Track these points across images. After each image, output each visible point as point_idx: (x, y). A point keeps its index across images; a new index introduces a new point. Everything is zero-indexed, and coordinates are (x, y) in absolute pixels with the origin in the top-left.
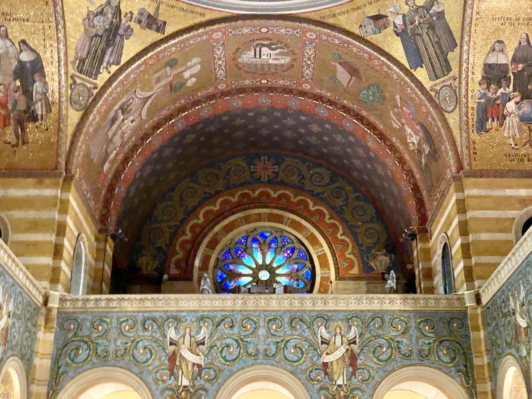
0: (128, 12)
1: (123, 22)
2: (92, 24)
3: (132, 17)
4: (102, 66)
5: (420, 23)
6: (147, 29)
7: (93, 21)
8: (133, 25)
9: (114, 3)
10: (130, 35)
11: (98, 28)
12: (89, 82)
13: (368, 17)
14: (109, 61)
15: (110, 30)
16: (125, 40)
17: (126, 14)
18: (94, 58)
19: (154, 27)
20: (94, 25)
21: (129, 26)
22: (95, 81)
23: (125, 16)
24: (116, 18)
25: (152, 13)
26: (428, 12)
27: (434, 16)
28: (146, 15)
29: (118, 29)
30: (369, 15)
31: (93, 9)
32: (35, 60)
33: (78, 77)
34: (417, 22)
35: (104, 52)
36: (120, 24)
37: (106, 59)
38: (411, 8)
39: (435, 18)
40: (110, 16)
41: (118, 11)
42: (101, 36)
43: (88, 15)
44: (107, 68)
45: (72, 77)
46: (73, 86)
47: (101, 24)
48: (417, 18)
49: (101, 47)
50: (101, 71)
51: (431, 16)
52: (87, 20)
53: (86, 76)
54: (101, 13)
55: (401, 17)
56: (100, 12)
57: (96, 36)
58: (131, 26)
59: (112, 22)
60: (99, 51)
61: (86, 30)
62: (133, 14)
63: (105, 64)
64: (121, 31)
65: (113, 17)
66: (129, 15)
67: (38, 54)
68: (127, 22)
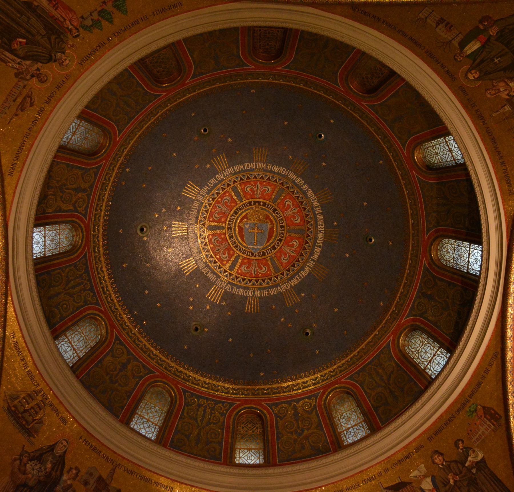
0: (73, 466)
1: (65, 477)
2: (22, 468)
5: (455, 482)
7: (25, 465)
9: (58, 451)
11: (30, 476)
13: (386, 488)
20: (25, 470)
24: (56, 471)
25: (105, 477)
26: (464, 466)
27: (472, 468)
29: (56, 486)
30: (387, 485)
31: (29, 449)
34: (452, 481)
36: (59, 480)
38: (441, 466)
39: (474, 471)
40: (49, 465)
41: (60, 462)
43: (21, 455)
48: (450, 476)
51: (469, 469)
54: (39, 457)
55: (429, 480)
57: (25, 485)
62: (79, 471)
65: (53, 469)
66: (74, 471)
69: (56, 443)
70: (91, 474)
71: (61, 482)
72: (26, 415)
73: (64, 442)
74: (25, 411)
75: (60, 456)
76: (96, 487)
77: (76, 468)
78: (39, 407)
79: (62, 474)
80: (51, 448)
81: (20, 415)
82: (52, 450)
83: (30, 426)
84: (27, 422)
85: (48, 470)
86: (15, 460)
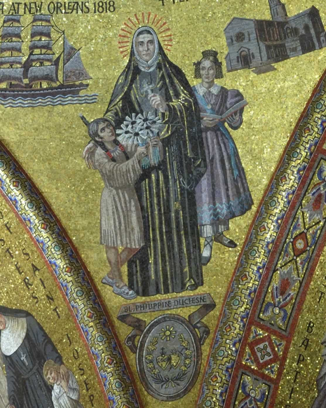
1: (201, 91)
2: (117, 153)
3: (217, 64)
4: (202, 241)
6: (275, 65)
7: (116, 142)
8: (238, 81)
9: (148, 62)
10: (242, 110)
11: (141, 149)
12: (183, 303)
14: (216, 215)
15: (177, 133)
16: (234, 133)
17: (198, 65)
18: (169, 232)
19: (291, 43)
21: (223, 91)
22: (200, 290)
23: (198, 75)
25: (267, 16)
28: (251, 30)
29: (199, 119)
31: (95, 112)
32: (27, 337)
33: (143, 306)
35: (190, 201)
36: (196, 103)
37: (205, 214)
40: (156, 100)
41: (171, 75)
42: (162, 166)
44: (218, 238)
45: (122, 318)
46: (138, 339)
47: (140, 138)
49: (175, 189)
50: (206, 253)
52: (99, 151)
53: (167, 291)
54: (127, 106)
56: (123, 109)
57: (146, 173)
58: (228, 87)
59: (171, 109)
60: (175, 205)
61: (108, 178)
62: (215, 54)
63: (208, 231)
64: (208, 118)
65: (168, 98)
66: (207, 63)
67: (27, 314)
68: (211, 84)
69: (132, 54)
70: (240, 37)
71: (201, 103)
72: (36, 69)
73: (141, 38)
74: (27, 66)
75: (159, 67)
76: (268, 47)
77: (206, 54)
78: (41, 34)
79: (191, 91)
80: (133, 71)
81: (26, 81)
82: (137, 71)
83: (60, 78)
84: (47, 78)
85: (161, 110)
86: (91, 153)
